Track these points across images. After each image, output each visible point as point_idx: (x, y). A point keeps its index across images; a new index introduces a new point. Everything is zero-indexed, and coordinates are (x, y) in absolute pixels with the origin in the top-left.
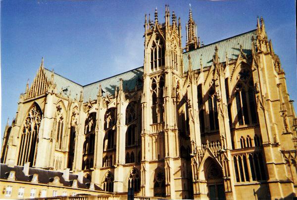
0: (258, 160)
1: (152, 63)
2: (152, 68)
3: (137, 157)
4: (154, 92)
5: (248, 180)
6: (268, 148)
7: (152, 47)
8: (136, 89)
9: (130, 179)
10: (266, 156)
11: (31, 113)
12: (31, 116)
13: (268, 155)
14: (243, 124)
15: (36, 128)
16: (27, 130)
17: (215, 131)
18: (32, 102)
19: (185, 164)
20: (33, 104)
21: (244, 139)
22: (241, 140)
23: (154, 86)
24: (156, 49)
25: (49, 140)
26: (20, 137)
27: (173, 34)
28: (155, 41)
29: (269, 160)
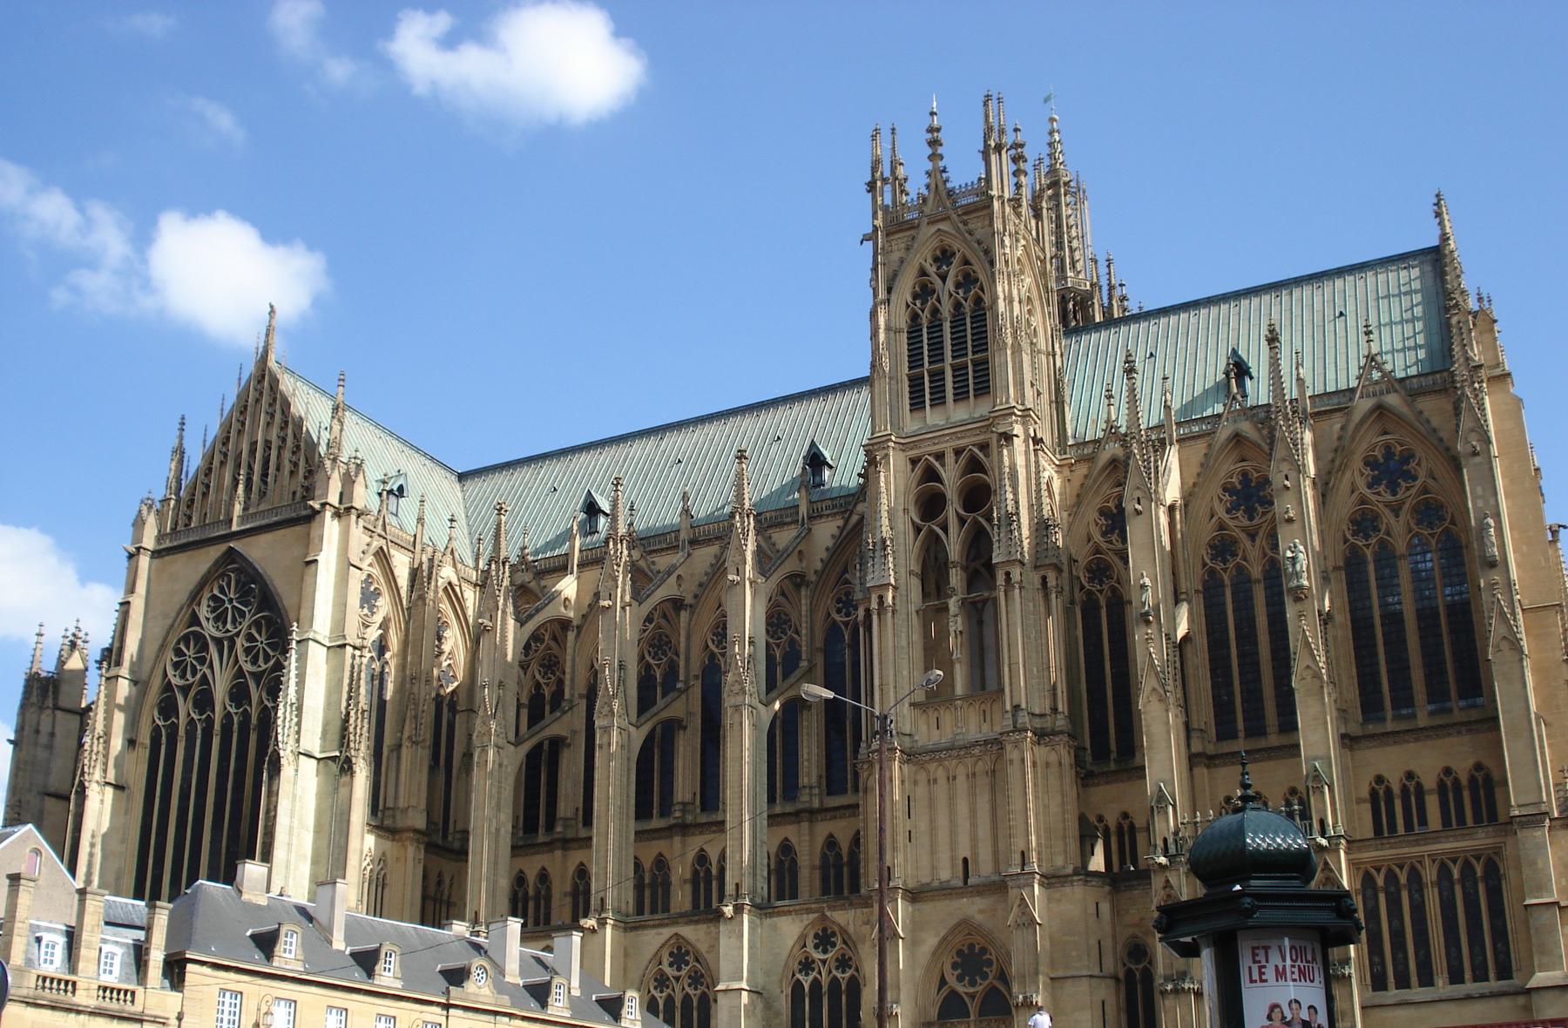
0: (1481, 888)
1: (916, 384)
2: (917, 404)
3: (813, 868)
4: (931, 531)
5: (1427, 979)
6: (1538, 834)
7: (915, 296)
8: (803, 510)
9: (798, 976)
10: (1526, 872)
11: (204, 612)
12: (210, 629)
13: (1535, 863)
14: (1384, 719)
15: (239, 694)
16: (184, 707)
17: (1274, 740)
18: (216, 552)
19: (1105, 907)
20: (218, 563)
21: (1389, 791)
22: (1374, 794)
23: (930, 504)
24: (935, 311)
25: (334, 768)
26: (145, 738)
27: (1023, 242)
28: (932, 270)
29: (1541, 887)
